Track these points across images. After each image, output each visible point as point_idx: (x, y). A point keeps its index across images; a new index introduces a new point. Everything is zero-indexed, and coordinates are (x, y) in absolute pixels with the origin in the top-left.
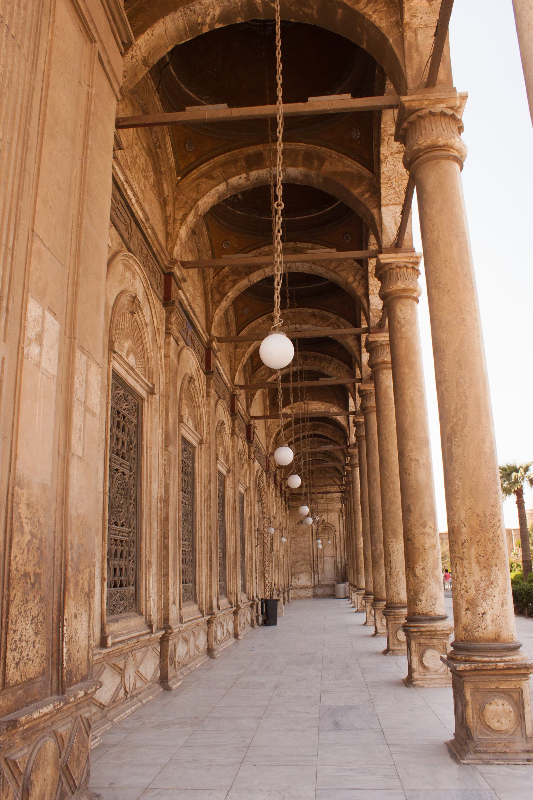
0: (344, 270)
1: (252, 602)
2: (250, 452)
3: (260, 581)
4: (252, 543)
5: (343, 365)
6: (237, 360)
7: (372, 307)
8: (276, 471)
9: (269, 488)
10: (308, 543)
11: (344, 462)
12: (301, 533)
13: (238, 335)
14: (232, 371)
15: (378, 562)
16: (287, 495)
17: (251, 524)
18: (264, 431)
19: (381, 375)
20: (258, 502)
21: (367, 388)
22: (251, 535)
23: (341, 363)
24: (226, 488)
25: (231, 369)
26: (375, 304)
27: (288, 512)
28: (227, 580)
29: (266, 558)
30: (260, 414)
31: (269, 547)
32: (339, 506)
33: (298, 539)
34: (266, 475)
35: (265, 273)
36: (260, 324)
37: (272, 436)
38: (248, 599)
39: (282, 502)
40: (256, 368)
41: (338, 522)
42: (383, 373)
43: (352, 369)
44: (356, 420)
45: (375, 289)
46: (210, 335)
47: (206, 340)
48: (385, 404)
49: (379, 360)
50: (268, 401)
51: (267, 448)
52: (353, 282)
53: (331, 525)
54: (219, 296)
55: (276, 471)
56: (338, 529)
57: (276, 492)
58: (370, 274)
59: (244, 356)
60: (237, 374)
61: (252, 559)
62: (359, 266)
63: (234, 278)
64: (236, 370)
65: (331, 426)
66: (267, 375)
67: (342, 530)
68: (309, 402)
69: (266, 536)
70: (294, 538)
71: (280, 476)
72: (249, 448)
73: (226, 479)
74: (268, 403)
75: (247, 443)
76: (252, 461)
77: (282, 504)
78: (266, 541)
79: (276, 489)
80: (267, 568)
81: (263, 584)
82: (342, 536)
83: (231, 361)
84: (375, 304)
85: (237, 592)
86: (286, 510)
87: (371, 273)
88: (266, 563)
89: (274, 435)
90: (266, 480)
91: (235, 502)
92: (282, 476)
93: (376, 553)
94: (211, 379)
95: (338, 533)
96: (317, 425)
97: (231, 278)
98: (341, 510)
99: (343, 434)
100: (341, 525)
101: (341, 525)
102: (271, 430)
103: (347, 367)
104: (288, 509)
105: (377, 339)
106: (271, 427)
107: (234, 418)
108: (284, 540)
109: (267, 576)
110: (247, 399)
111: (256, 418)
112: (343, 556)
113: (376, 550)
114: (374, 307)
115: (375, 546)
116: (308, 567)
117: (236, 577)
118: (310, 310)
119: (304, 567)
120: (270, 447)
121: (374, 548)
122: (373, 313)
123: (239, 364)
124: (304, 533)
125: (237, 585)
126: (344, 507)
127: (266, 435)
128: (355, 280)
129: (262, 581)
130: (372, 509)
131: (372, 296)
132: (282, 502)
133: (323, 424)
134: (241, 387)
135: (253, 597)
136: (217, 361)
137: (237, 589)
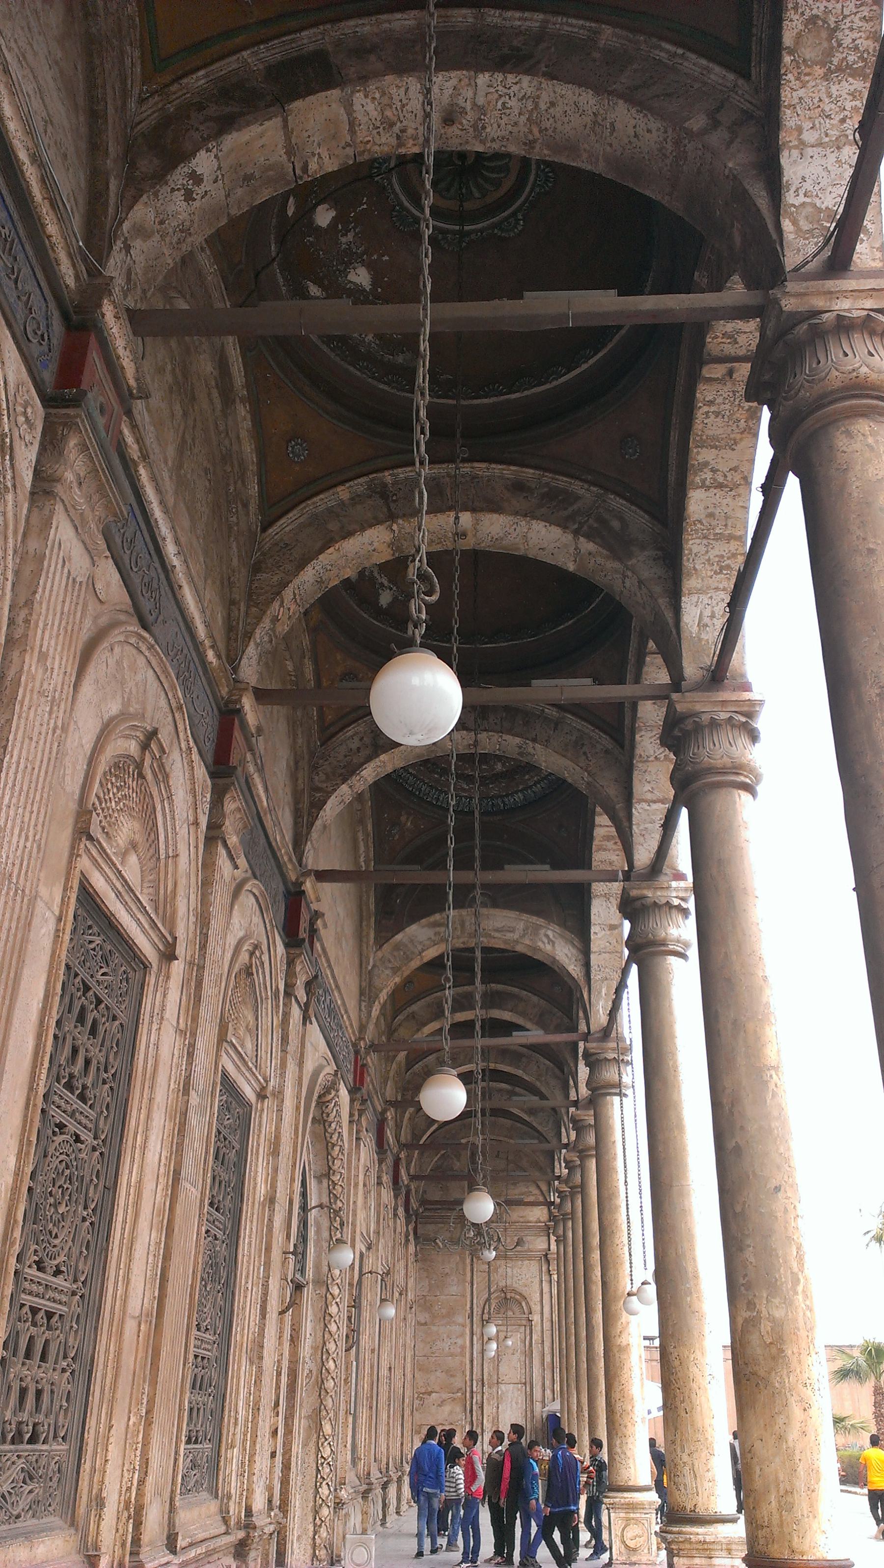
0: (669, 95)
1: (241, 1534)
2: (290, 974)
3: (305, 1445)
4: (265, 1294)
5: (596, 734)
6: (257, 605)
7: (790, 198)
8: (384, 1111)
9: (358, 1146)
10: (460, 1342)
11: (554, 1142)
12: (444, 1311)
13: (264, 529)
14: (234, 639)
15: (767, 1383)
16: (414, 1204)
17: (270, 1220)
18: (357, 979)
19: (841, 441)
20: (319, 1179)
21: (699, 708)
22: (267, 1265)
23: (588, 728)
24: (145, 1017)
25: (230, 628)
26: (808, 186)
27: (412, 1248)
28: (90, 1438)
29: (331, 1365)
30: (336, 864)
31: (344, 1331)
32: (540, 1244)
33: (434, 1328)
34: (352, 1101)
35: (352, 131)
36: (342, 504)
37: (377, 997)
38: (225, 1521)
39: (395, 1209)
40: (332, 730)
41: (536, 1286)
42: (849, 434)
43: (622, 746)
44: (634, 893)
45: (807, 125)
46: (93, 273)
47: (71, 281)
48: (871, 551)
49: (835, 378)
50: (372, 900)
51: (362, 1028)
52: (704, 132)
53: (520, 1294)
54: (156, 161)
55: (384, 1111)
56: (536, 1308)
57: (380, 1170)
58: (787, 59)
59: (279, 593)
60: (251, 651)
61: (261, 1358)
62: (731, 76)
63: (228, 109)
64: (248, 635)
65: (535, 999)
66: (364, 753)
67: (547, 1309)
68: (484, 911)
69: (335, 1291)
70: (425, 1324)
71: (397, 1138)
72: (290, 963)
73: (151, 979)
74: (372, 907)
75: (287, 946)
76: (296, 1013)
77: (395, 1215)
78: (333, 1309)
79: (381, 1162)
80: (329, 1403)
81: (313, 1457)
82: (547, 1325)
83: (233, 602)
84: (808, 186)
85: (140, 1494)
86: (407, 1241)
87: (791, 52)
88: (330, 1384)
89: (383, 996)
90: (351, 1115)
91: (186, 1091)
92: (403, 1139)
93: (754, 1338)
94: (70, 424)
95: (536, 1318)
96: (498, 993)
97: (213, 110)
98: (546, 1255)
99: (566, 1020)
100: (546, 1297)
101: (546, 1297)
102: (377, 982)
103: (605, 741)
104: (411, 1238)
105: (819, 303)
106: (376, 971)
107: (221, 781)
108: (390, 1311)
109: (327, 1429)
110: (297, 814)
111: (322, 876)
112: (548, 1383)
113: (752, 1323)
114: (801, 199)
115: (751, 1305)
116: (458, 1409)
117: (149, 1424)
118: (509, 472)
119: (447, 1408)
120: (371, 1027)
121: (744, 1314)
122: (795, 223)
123: (259, 619)
124: (451, 1313)
125: (145, 1462)
126: (553, 1247)
127: (362, 993)
128: (715, 124)
129: (312, 1445)
130: (730, 1145)
131: (795, 153)
132: (395, 1209)
133: (516, 990)
134: (261, 695)
135: (249, 1512)
136: (142, 471)
137: (142, 1482)
